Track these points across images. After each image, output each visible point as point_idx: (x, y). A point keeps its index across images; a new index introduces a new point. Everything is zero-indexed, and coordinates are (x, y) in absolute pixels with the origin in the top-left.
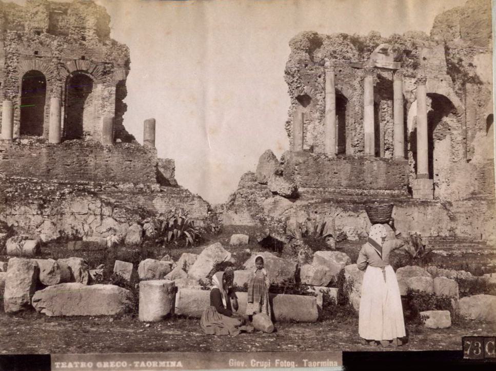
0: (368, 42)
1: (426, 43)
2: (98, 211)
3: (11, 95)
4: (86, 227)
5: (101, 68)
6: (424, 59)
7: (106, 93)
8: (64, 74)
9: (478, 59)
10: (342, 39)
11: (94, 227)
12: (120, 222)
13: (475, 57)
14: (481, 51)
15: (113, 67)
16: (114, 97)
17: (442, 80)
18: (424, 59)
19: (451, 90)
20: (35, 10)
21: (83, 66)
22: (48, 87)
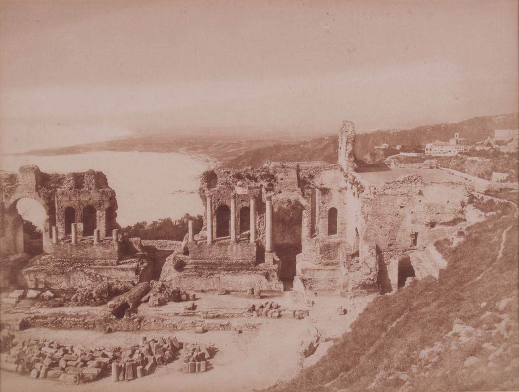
0: (243, 173)
1: (283, 170)
2: (84, 278)
3: (61, 219)
4: (79, 283)
5: (98, 203)
6: (282, 179)
7: (101, 214)
8: (82, 207)
9: (325, 174)
10: (227, 174)
11: (82, 283)
12: (93, 281)
13: (323, 173)
14: (327, 168)
15: (103, 202)
16: (104, 216)
17: (293, 191)
18: (282, 179)
19: (300, 196)
20: (69, 179)
21: (90, 203)
22: (76, 214)
